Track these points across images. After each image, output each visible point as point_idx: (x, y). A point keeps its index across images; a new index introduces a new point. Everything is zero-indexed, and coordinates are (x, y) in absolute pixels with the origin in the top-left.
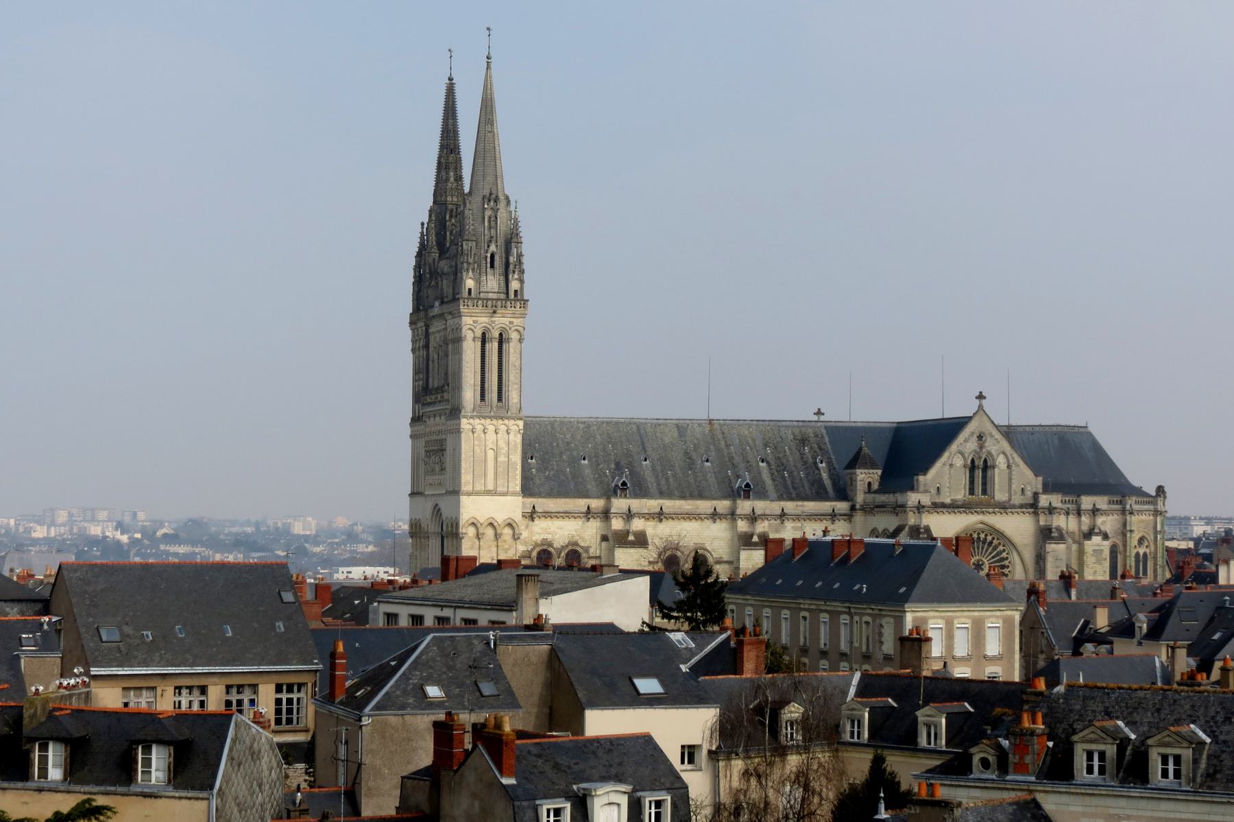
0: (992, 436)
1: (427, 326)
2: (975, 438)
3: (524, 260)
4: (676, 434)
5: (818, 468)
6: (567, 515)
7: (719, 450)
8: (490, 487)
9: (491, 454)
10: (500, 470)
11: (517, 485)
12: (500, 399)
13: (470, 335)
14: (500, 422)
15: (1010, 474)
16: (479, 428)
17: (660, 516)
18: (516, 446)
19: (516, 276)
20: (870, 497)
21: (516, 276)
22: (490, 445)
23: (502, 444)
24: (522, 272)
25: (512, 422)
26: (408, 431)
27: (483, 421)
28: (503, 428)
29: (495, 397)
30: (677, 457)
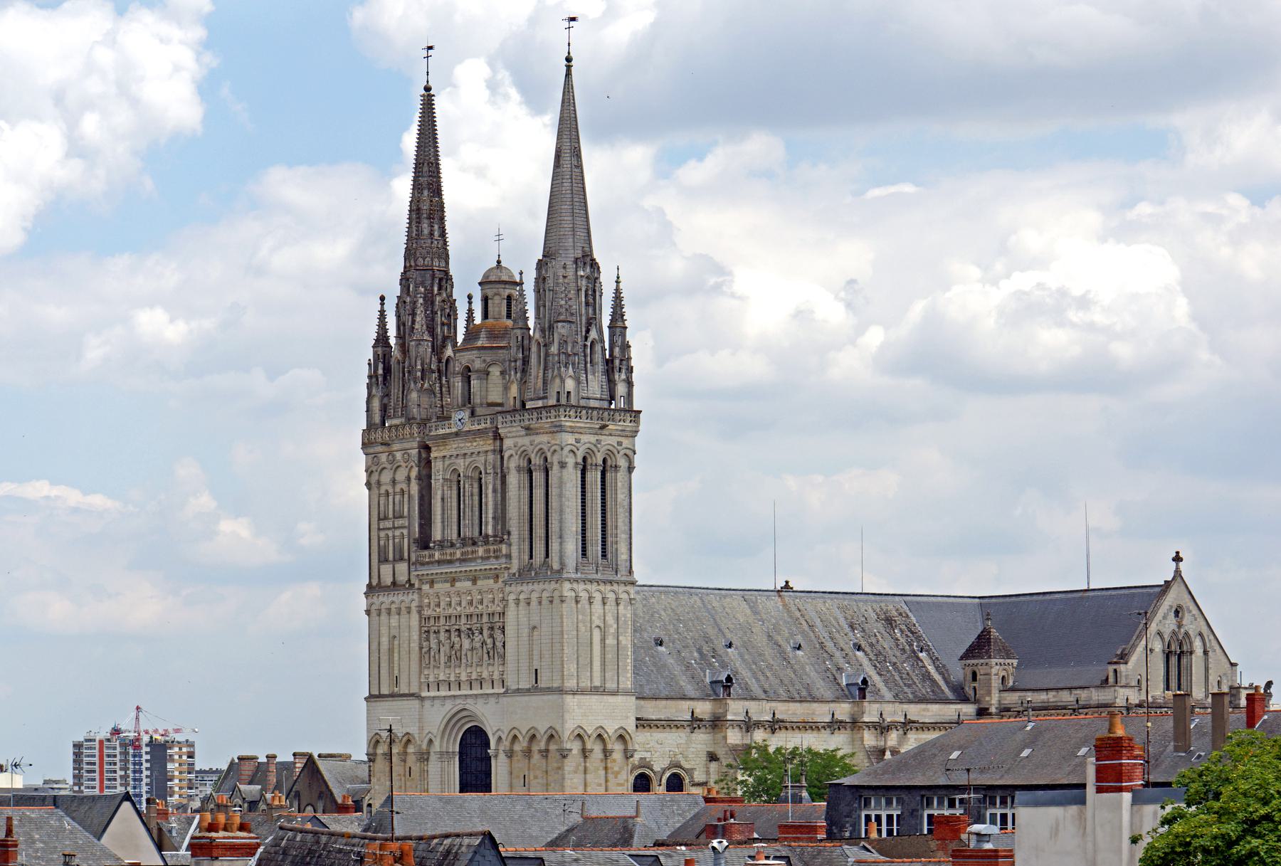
2: (1172, 614)
3: (634, 353)
4: (748, 611)
5: (918, 658)
6: (669, 724)
8: (597, 683)
9: (597, 635)
10: (609, 656)
11: (627, 682)
12: (604, 555)
14: (609, 587)
16: (584, 595)
17: (775, 725)
18: (625, 622)
19: (623, 376)
20: (1012, 698)
22: (597, 622)
23: (610, 620)
24: (630, 370)
26: (363, 603)
27: (588, 586)
28: (611, 596)
30: (760, 640)
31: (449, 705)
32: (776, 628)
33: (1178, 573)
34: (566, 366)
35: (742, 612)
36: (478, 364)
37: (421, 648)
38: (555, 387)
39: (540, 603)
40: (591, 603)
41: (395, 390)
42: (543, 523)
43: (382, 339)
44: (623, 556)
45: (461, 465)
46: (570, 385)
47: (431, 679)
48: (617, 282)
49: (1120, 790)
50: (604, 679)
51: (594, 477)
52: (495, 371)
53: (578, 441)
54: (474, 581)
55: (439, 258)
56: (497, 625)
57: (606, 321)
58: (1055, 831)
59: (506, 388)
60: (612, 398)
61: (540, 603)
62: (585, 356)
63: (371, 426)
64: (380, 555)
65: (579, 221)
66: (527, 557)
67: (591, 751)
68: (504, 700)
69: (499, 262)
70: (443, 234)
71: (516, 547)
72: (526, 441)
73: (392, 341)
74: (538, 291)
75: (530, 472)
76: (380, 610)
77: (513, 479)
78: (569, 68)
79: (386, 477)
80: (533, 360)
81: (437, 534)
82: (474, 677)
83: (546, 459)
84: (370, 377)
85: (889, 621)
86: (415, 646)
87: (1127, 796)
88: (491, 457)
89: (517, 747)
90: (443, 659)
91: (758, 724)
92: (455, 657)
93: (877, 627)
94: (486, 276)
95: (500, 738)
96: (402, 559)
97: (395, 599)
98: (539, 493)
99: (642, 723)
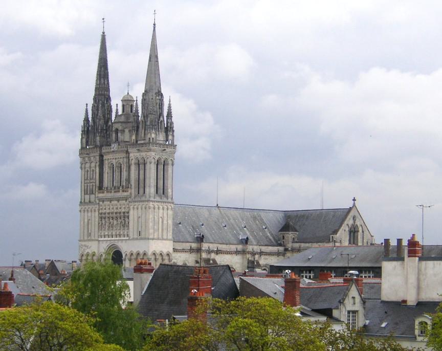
0: (358, 218)
1: (101, 156)
2: (352, 219)
6: (183, 251)
9: (160, 220)
11: (170, 237)
12: (163, 194)
14: (165, 204)
15: (363, 235)
16: (156, 206)
17: (218, 252)
19: (171, 133)
20: (297, 245)
22: (161, 215)
24: (173, 131)
25: (169, 204)
26: (78, 208)
27: (158, 204)
28: (166, 207)
29: (162, 191)
31: (108, 243)
33: (354, 205)
34: (152, 129)
36: (120, 128)
37: (99, 223)
38: (149, 136)
39: (142, 209)
40: (159, 209)
41: (91, 136)
42: (143, 182)
43: (86, 119)
44: (170, 194)
45: (114, 162)
47: (102, 234)
48: (170, 101)
49: (416, 256)
50: (162, 236)
51: (161, 167)
52: (127, 131)
54: (118, 201)
55: (107, 91)
56: (126, 216)
57: (165, 114)
58: (395, 268)
59: (131, 136)
60: (167, 140)
61: (142, 209)
62: (158, 126)
63: (82, 148)
64: (86, 191)
66: (137, 193)
67: (158, 259)
68: (128, 241)
69: (128, 93)
70: (108, 84)
71: (133, 191)
72: (138, 154)
73: (90, 119)
74: (142, 104)
75: (139, 165)
76: (84, 210)
77: (133, 168)
78: (154, 28)
79: (88, 165)
80: (140, 126)
81: (106, 183)
82: (118, 233)
83: (144, 160)
84: (82, 131)
86: (97, 223)
87: (417, 258)
88: (125, 160)
89: (133, 257)
90: (107, 228)
91: (213, 251)
92: (111, 226)
94: (124, 97)
95: (126, 254)
96: (93, 193)
97: (90, 207)
98: (142, 172)
99: (175, 250)
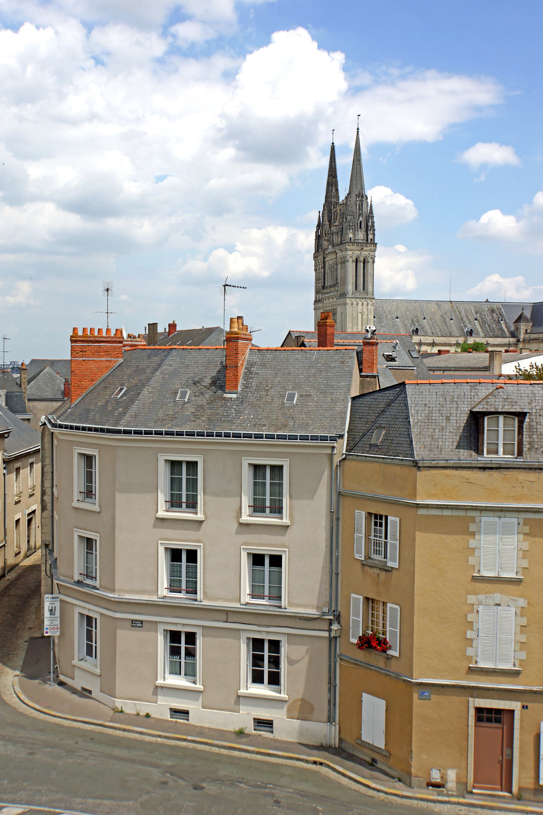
1: (324, 258)
3: (375, 225)
5: (500, 323)
7: (456, 315)
9: (360, 315)
10: (364, 322)
12: (364, 289)
13: (351, 260)
16: (355, 303)
18: (371, 311)
19: (371, 232)
20: (527, 336)
21: (371, 232)
23: (365, 310)
24: (374, 230)
26: (313, 307)
28: (365, 303)
30: (438, 317)
32: (446, 313)
34: (350, 229)
35: (434, 308)
46: (351, 235)
53: (353, 253)
65: (359, 182)
72: (341, 254)
78: (358, 132)
81: (326, 285)
85: (493, 311)
93: (486, 313)
